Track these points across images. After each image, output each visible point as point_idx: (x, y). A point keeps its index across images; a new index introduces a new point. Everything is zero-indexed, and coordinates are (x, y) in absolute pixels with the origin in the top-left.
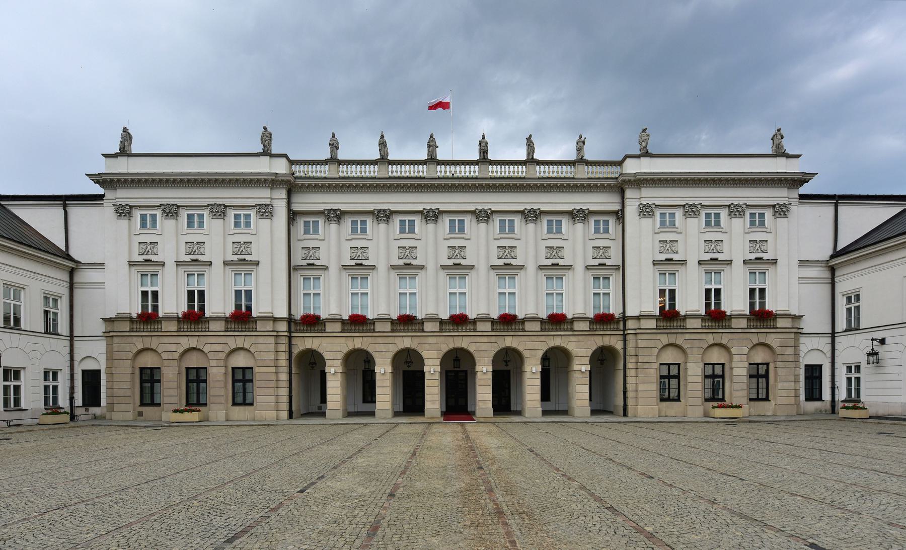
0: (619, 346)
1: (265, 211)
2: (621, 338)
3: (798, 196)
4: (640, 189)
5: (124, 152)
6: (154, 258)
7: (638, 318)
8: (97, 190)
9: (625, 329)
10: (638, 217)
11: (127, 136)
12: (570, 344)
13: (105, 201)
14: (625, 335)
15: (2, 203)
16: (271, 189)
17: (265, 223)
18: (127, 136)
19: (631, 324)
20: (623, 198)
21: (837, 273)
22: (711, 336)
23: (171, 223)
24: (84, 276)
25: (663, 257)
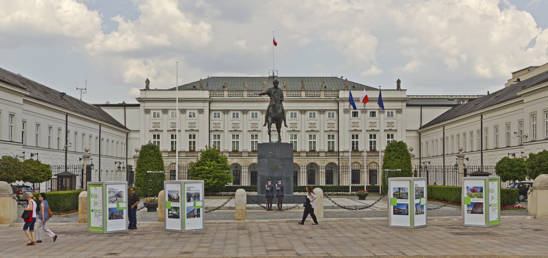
0: (337, 163)
1: (201, 111)
2: (338, 159)
3: (406, 105)
4: (344, 102)
5: (147, 89)
6: (159, 129)
7: (343, 152)
8: (137, 103)
9: (339, 156)
10: (343, 113)
11: (148, 82)
12: (318, 163)
13: (140, 107)
14: (339, 158)
15: (101, 107)
16: (203, 102)
17: (201, 115)
18: (148, 82)
19: (341, 154)
20: (338, 105)
21: (422, 135)
22: (371, 159)
23: (165, 116)
24: (132, 135)
25: (353, 129)
